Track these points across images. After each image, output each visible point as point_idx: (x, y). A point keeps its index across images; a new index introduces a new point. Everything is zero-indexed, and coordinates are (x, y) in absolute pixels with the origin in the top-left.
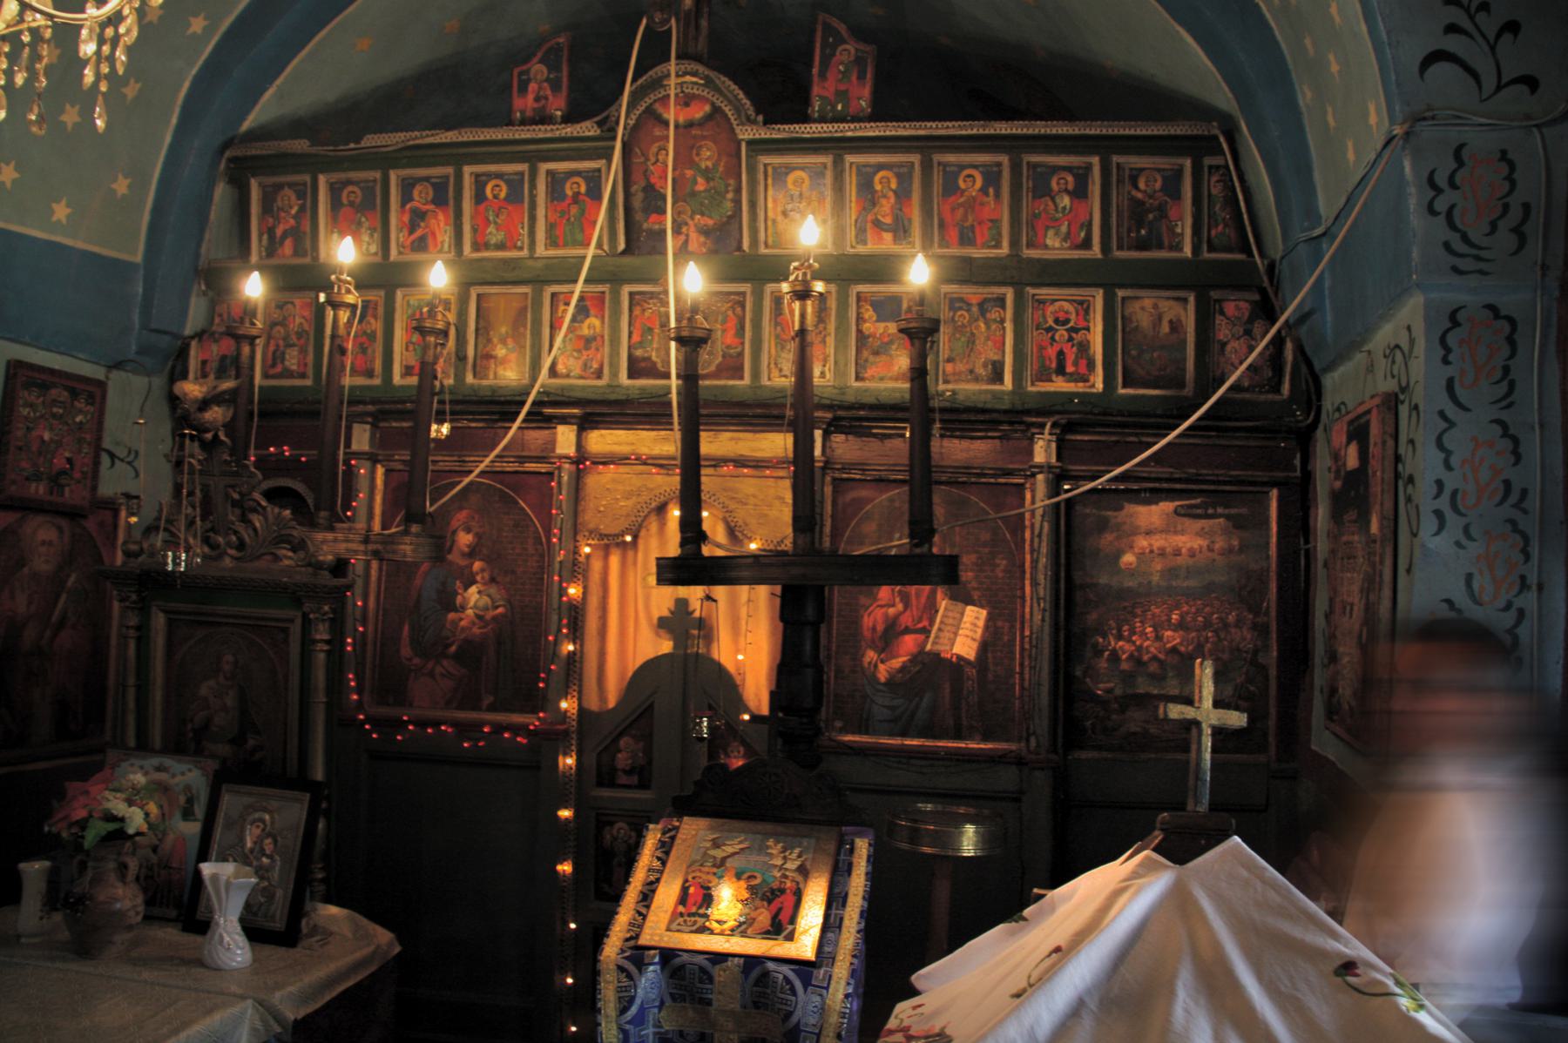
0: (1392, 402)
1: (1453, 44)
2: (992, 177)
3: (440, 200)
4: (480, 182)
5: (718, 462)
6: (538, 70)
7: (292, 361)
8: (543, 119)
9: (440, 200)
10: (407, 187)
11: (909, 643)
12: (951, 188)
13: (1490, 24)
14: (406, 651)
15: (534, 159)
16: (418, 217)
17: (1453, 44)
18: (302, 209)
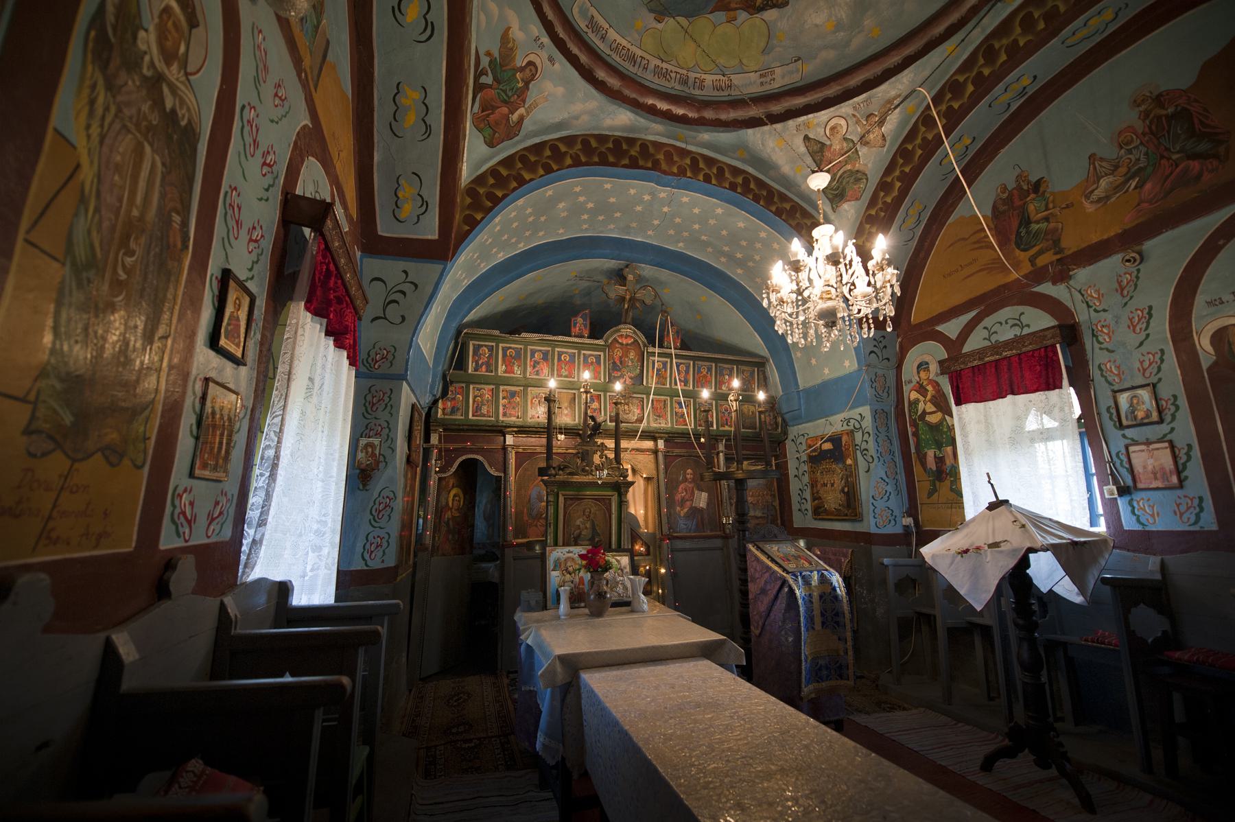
0: (851, 433)
1: (875, 349)
2: (710, 369)
3: (545, 358)
4: (560, 354)
5: (626, 450)
6: (580, 320)
7: (484, 410)
8: (582, 337)
9: (545, 358)
10: (533, 353)
11: (688, 503)
12: (699, 371)
13: (882, 345)
14: (526, 518)
15: (580, 349)
16: (537, 363)
17: (875, 349)
18: (490, 356)
